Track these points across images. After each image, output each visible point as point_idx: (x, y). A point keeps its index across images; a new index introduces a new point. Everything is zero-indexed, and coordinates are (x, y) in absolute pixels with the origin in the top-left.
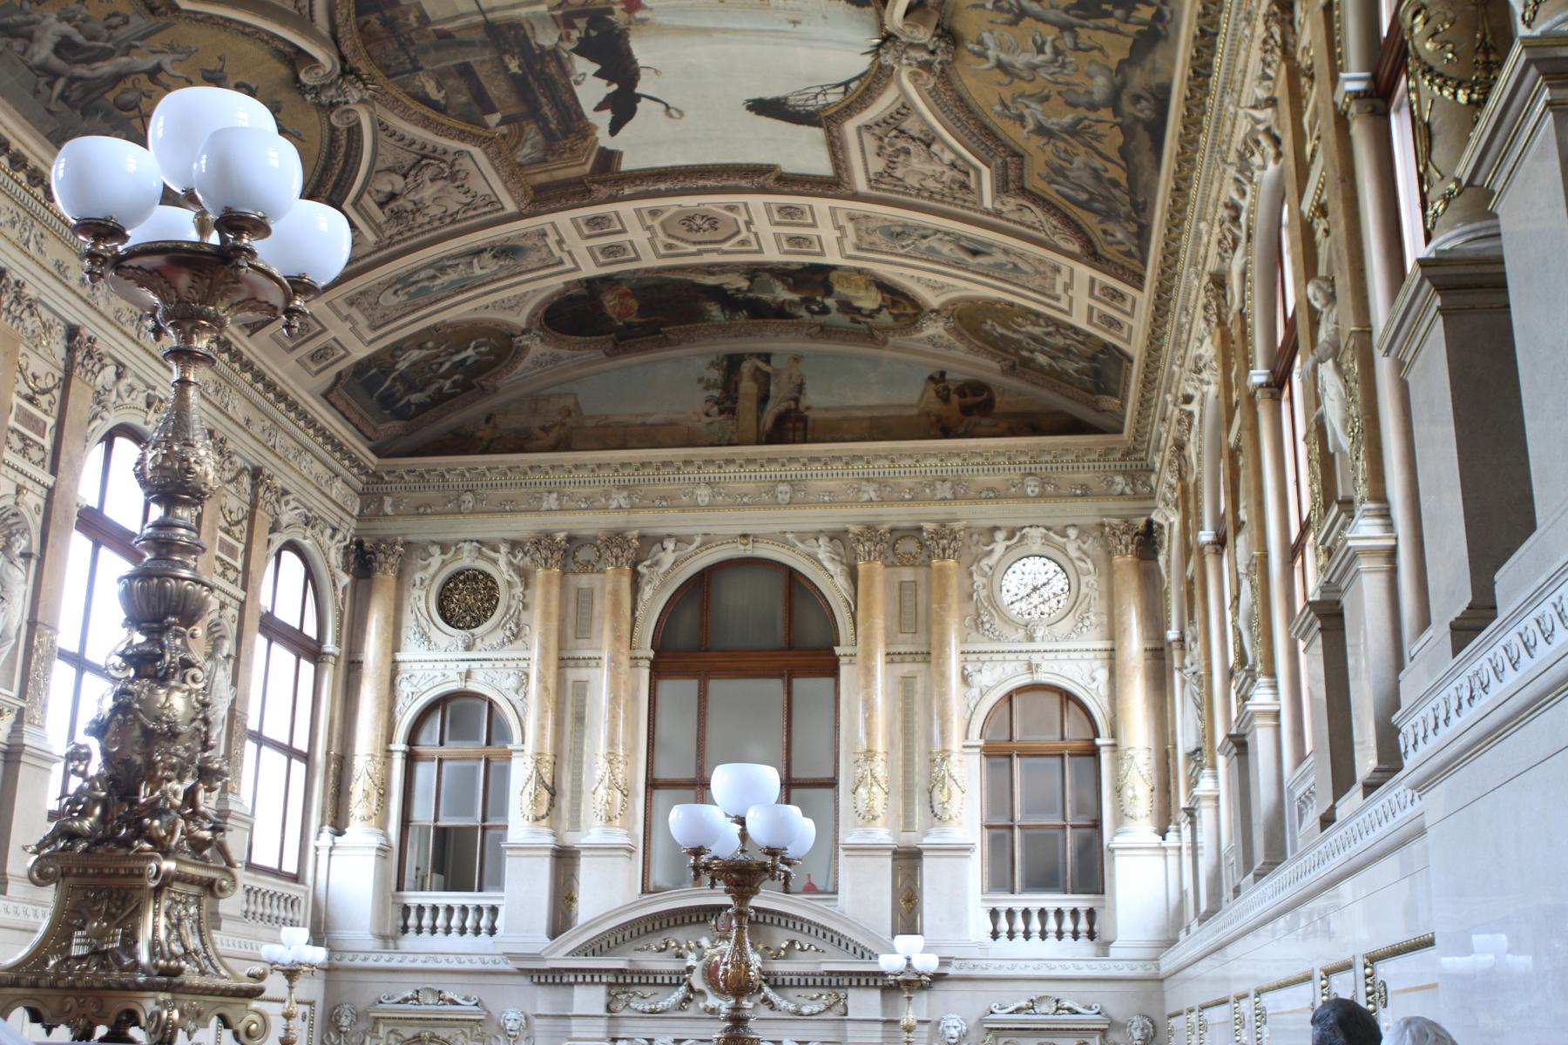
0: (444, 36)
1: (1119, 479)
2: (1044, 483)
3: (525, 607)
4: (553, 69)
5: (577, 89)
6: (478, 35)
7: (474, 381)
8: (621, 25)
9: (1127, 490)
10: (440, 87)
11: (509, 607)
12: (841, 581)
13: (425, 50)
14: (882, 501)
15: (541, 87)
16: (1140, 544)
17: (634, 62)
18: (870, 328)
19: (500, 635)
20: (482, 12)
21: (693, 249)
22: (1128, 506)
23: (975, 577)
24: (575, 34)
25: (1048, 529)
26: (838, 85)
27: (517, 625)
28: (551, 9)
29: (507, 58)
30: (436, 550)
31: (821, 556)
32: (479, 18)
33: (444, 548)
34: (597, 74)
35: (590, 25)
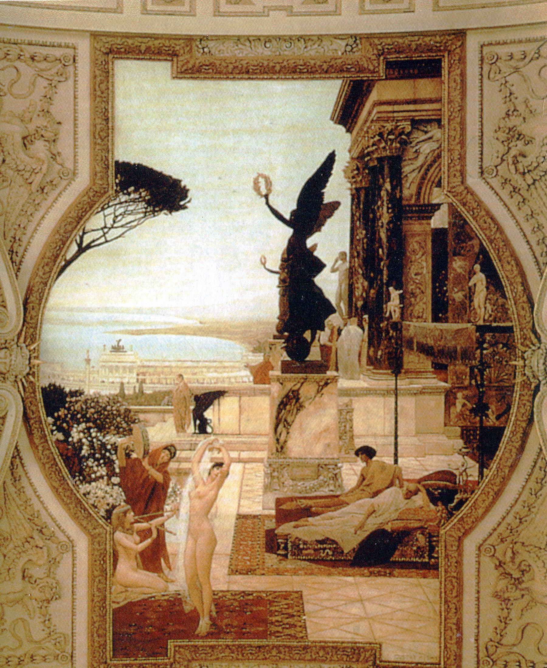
0: (440, 368)
4: (361, 284)
5: (346, 248)
6: (411, 359)
8: (281, 343)
10: (470, 295)
13: (466, 355)
15: (379, 260)
17: (282, 281)
20: (396, 392)
24: (323, 336)
26: (89, 247)
28: (335, 379)
29: (396, 317)
32: (403, 383)
34: (319, 266)
35: (306, 347)
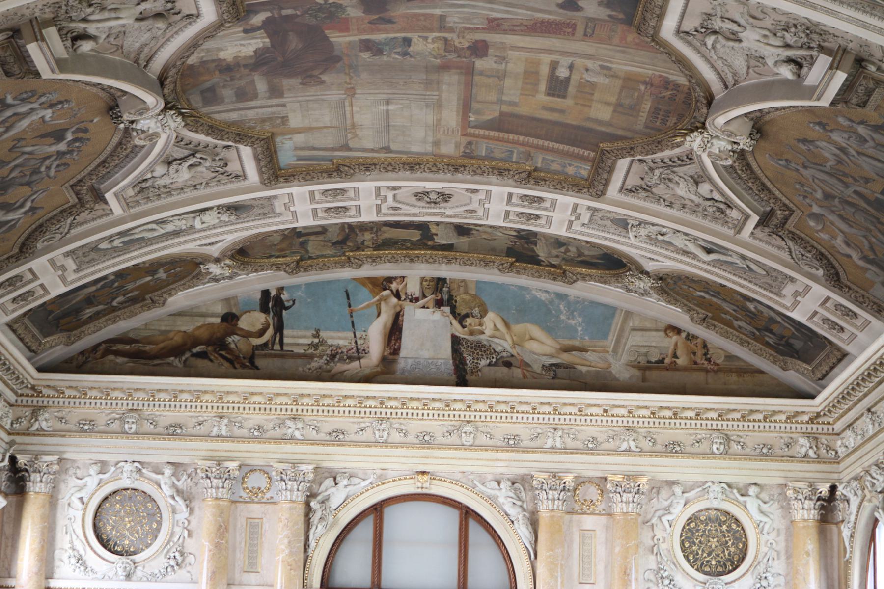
1: (803, 441)
2: (728, 438)
3: (190, 535)
7: (147, 297)
9: (811, 453)
11: (172, 534)
12: (524, 531)
14: (565, 450)
16: (822, 507)
18: (564, 272)
19: (161, 562)
21: (416, 210)
22: (809, 470)
23: (657, 531)
25: (729, 486)
27: (182, 554)
30: (93, 470)
31: (501, 500)
33: (103, 467)
